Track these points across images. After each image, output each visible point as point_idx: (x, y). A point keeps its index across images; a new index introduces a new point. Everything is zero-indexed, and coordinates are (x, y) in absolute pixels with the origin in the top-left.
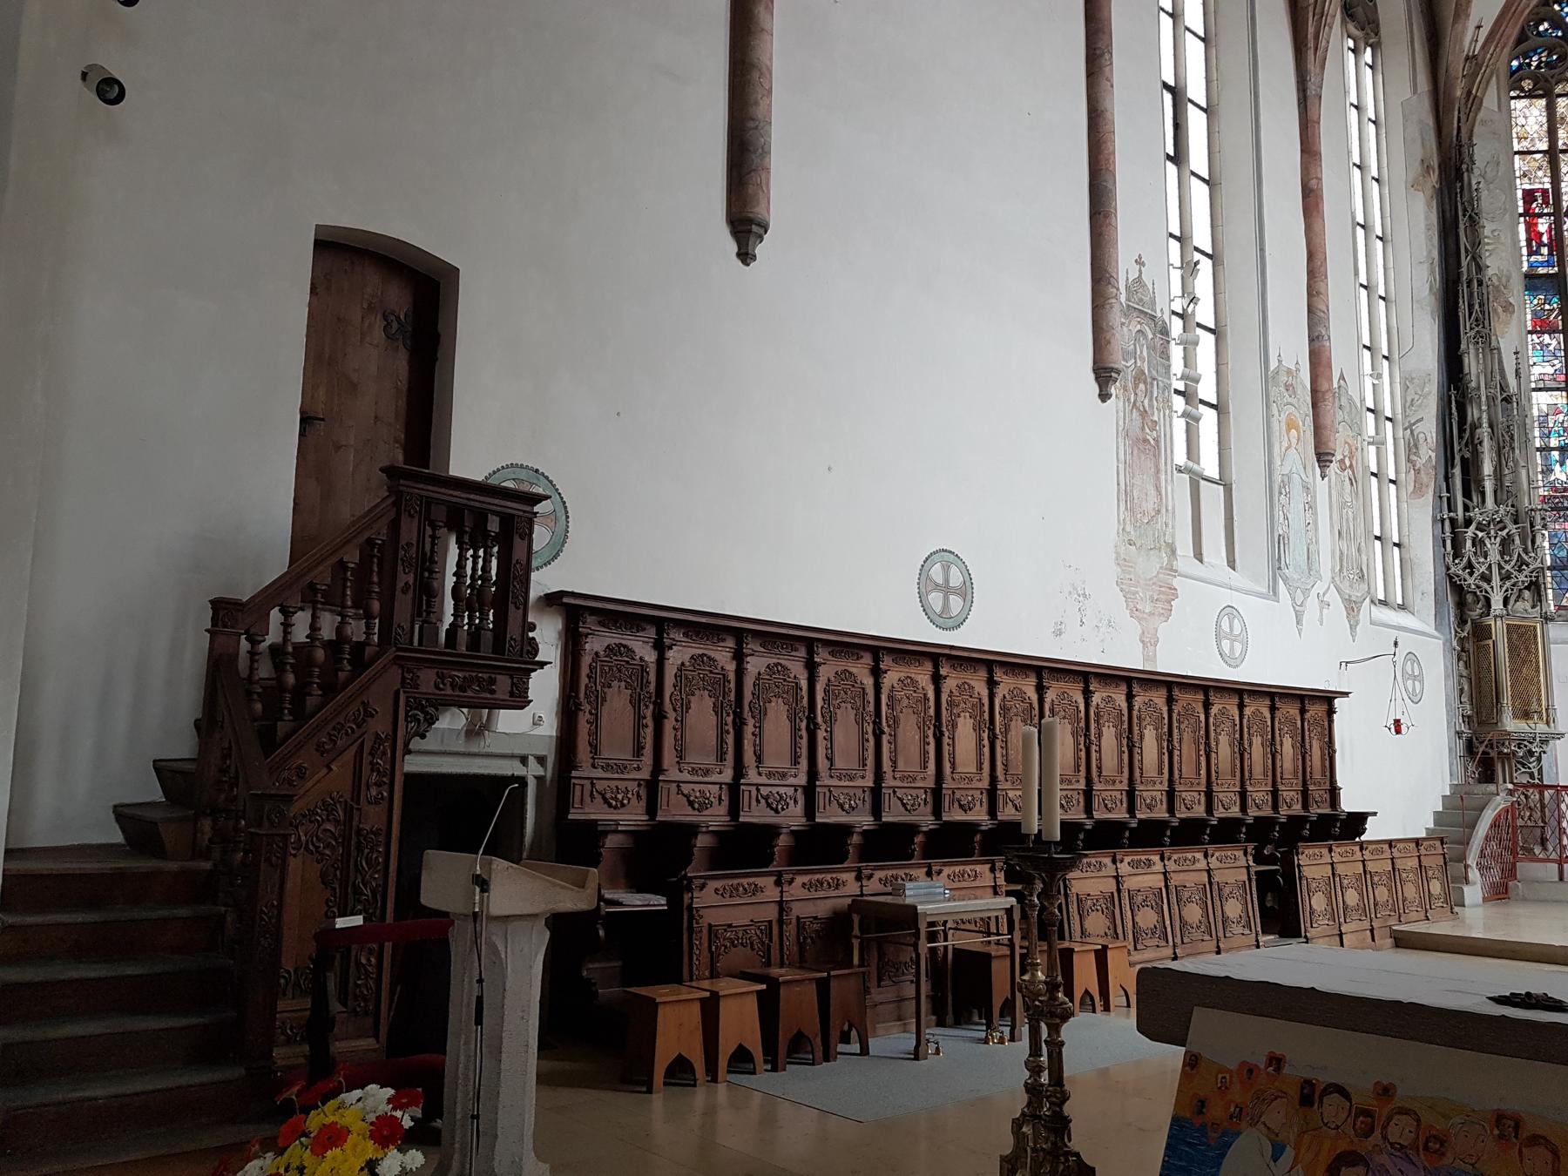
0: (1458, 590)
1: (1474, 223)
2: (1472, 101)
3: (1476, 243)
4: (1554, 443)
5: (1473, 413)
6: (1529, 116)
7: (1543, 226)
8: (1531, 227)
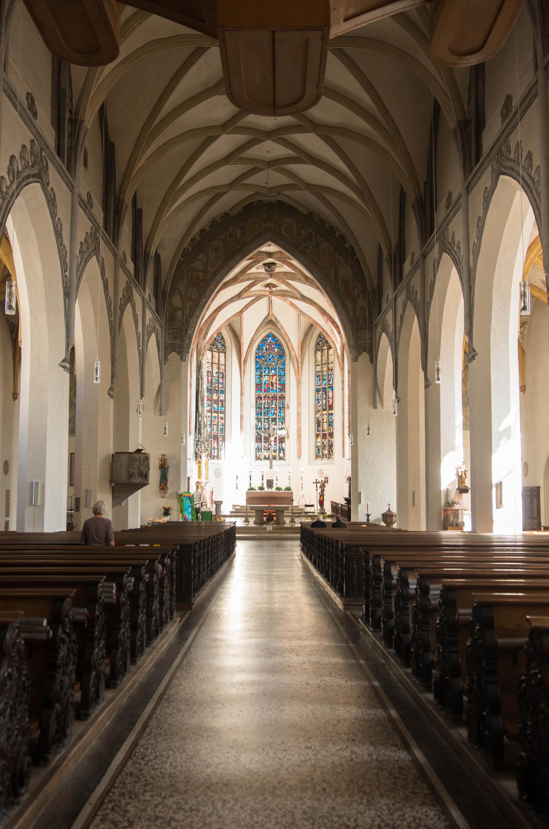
0: (196, 454)
1: (202, 379)
2: (203, 354)
3: (202, 384)
4: (208, 423)
5: (200, 419)
6: (208, 354)
7: (210, 378)
8: (208, 378)
